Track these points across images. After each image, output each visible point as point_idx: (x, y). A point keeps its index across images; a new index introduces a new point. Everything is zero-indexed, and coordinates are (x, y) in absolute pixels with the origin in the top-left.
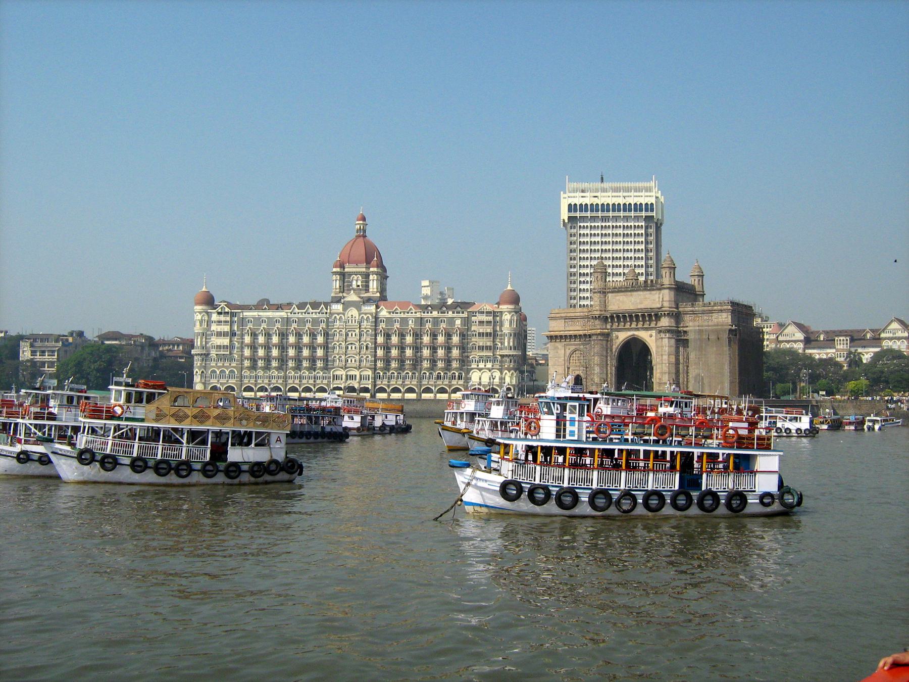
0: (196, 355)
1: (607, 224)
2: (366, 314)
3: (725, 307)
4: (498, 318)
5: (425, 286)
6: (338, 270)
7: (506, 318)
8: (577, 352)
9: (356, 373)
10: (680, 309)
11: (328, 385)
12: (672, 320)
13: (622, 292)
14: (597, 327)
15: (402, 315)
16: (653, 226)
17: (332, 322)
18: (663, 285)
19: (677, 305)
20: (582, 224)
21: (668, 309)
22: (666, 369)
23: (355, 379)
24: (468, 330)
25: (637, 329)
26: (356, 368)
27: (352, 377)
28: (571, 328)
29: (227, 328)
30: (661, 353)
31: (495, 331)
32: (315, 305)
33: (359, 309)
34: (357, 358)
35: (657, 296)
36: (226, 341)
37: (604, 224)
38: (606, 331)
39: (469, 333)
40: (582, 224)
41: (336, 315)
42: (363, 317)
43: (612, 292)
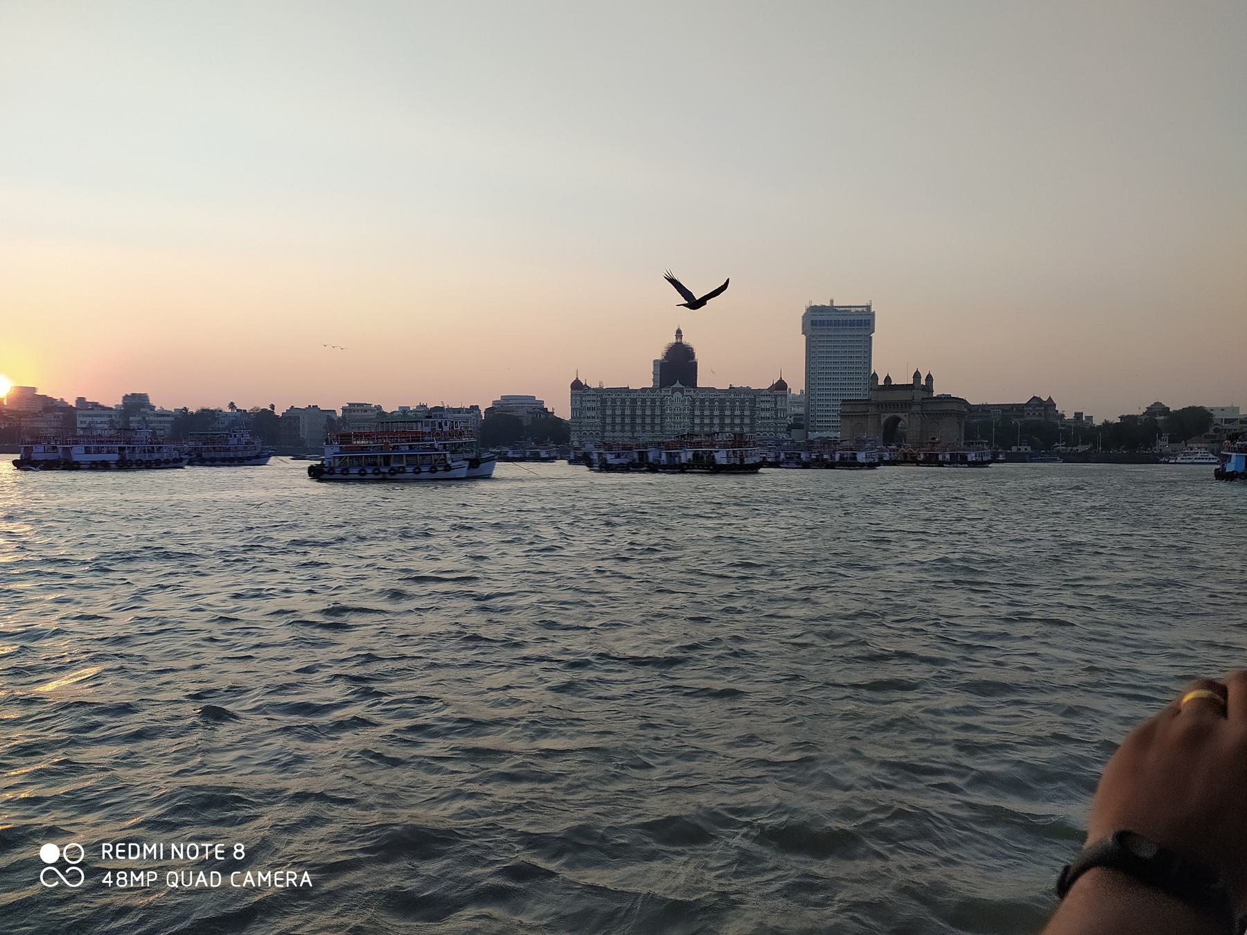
14: (872, 409)
33: (682, 393)
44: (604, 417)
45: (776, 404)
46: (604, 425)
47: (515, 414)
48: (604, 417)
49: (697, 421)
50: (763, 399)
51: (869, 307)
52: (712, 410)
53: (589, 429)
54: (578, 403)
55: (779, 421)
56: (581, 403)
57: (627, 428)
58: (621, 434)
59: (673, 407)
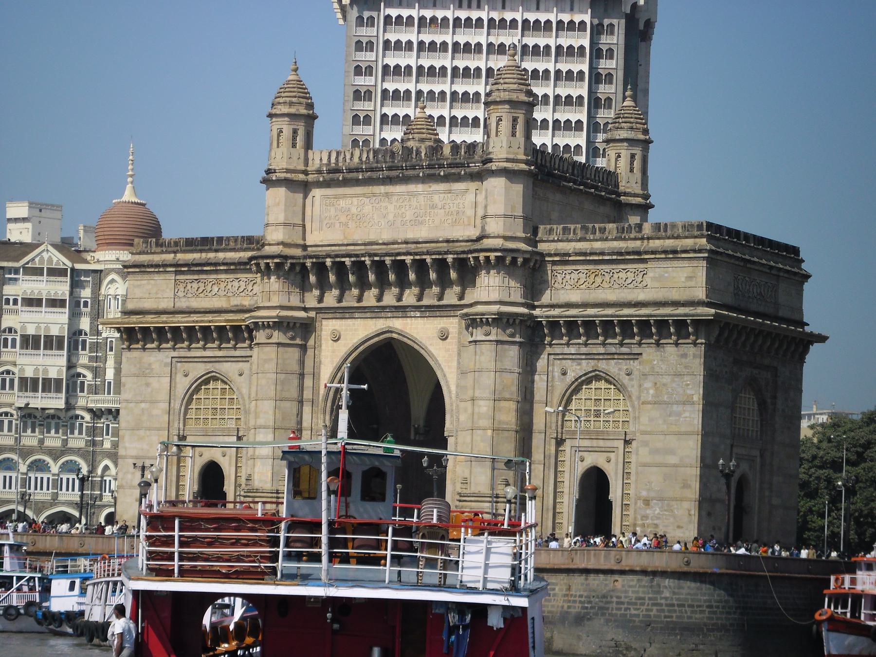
1: (474, 15)
3: (689, 243)
4: (86, 293)
5: (16, 220)
7: (111, 292)
8: (211, 386)
10: (542, 247)
12: (513, 283)
13: (357, 183)
16: (619, 24)
18: (490, 161)
19: (535, 231)
20: (394, 12)
21: (498, 243)
22: (483, 448)
25: (402, 310)
28: (195, 304)
30: (470, 393)
31: (74, 334)
35: (470, 197)
37: (463, 14)
38: (302, 314)
40: (394, 12)
43: (327, 184)
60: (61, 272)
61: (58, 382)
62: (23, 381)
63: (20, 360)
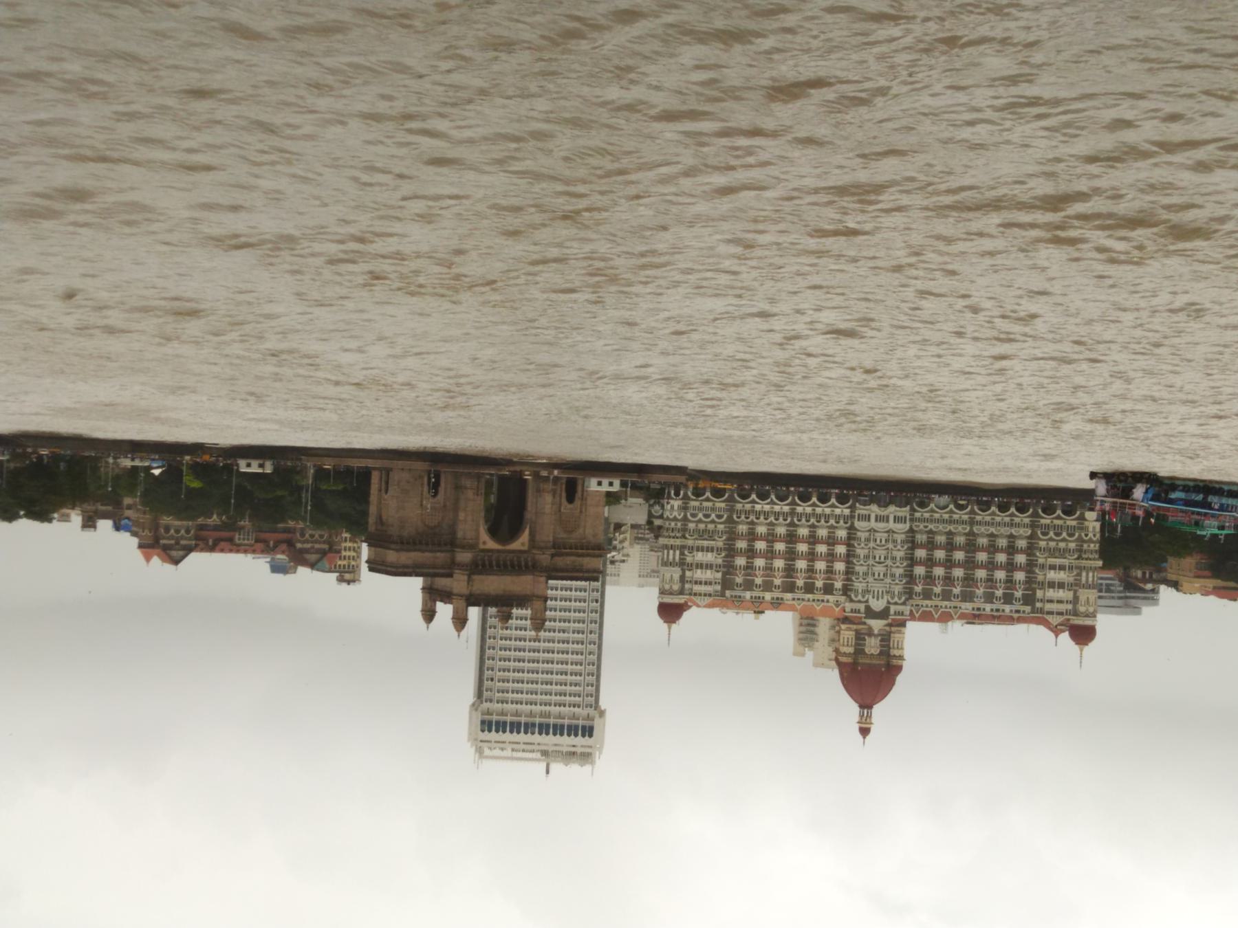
0: (1094, 559)
2: (860, 602)
6: (895, 662)
9: (873, 524)
11: (913, 510)
15: (810, 596)
17: (905, 593)
23: (877, 516)
24: (724, 574)
26: (875, 531)
27: (879, 519)
29: (1051, 594)
32: (926, 617)
33: (868, 608)
34: (872, 544)
36: (1052, 575)
39: (725, 570)
41: (900, 602)
42: (863, 597)
44: (1030, 567)
45: (683, 579)
46: (1030, 550)
47: (1219, 583)
48: (1030, 567)
49: (841, 549)
50: (709, 589)
51: (480, 751)
52: (811, 570)
53: (1062, 545)
54: (1082, 598)
55: (678, 542)
56: (1076, 600)
57: (983, 541)
58: (992, 530)
59: (888, 580)
60: (695, 594)
61: (698, 550)
62: (712, 551)
63: (713, 559)
